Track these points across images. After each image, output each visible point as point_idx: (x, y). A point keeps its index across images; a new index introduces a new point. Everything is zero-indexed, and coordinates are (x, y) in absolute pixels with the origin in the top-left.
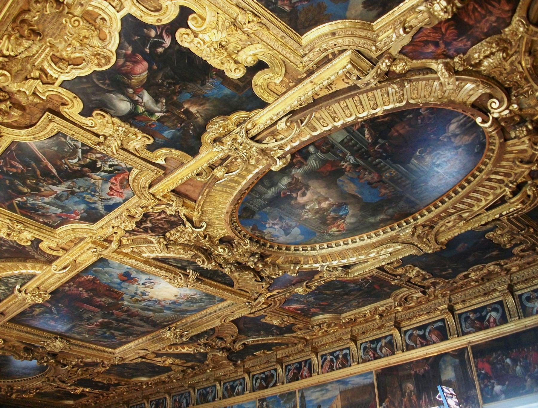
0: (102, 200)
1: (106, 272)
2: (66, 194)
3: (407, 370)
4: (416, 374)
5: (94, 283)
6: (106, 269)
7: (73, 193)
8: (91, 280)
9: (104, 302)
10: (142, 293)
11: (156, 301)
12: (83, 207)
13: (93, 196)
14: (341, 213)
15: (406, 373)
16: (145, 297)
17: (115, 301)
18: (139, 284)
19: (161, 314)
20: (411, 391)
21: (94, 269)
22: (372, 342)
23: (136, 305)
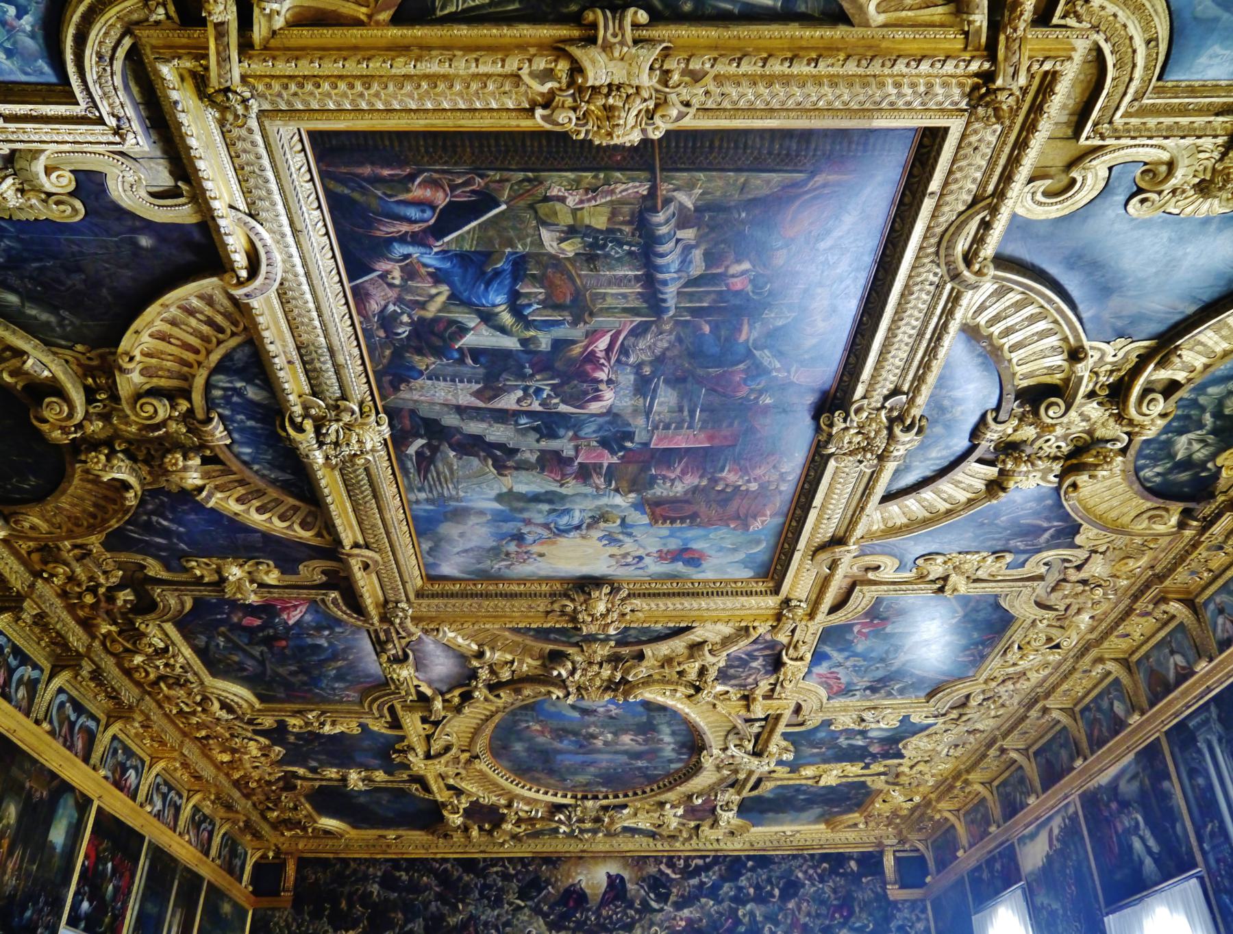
0: (840, 665)
1: (735, 550)
2: (891, 656)
3: (24, 772)
4: (30, 795)
5: (738, 517)
6: (741, 556)
7: (882, 660)
8: (750, 520)
9: (673, 481)
10: (620, 541)
11: (562, 532)
12: (860, 648)
13: (855, 666)
14: (566, 742)
15: (22, 777)
16: (596, 534)
17: (649, 494)
18: (648, 555)
19: (493, 493)
20: (8, 826)
21: (764, 545)
22: (17, 651)
23: (590, 504)
